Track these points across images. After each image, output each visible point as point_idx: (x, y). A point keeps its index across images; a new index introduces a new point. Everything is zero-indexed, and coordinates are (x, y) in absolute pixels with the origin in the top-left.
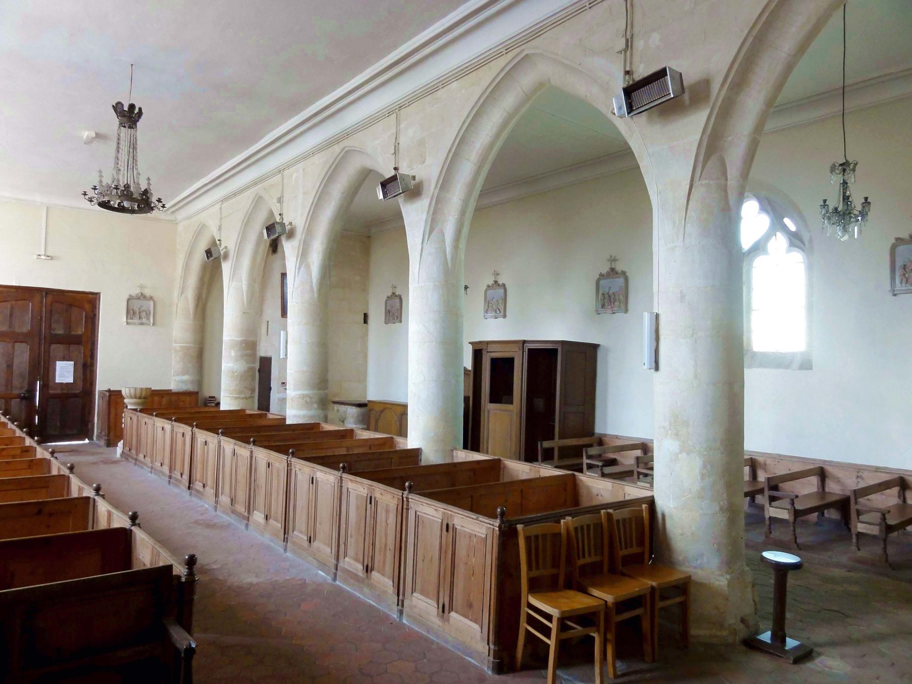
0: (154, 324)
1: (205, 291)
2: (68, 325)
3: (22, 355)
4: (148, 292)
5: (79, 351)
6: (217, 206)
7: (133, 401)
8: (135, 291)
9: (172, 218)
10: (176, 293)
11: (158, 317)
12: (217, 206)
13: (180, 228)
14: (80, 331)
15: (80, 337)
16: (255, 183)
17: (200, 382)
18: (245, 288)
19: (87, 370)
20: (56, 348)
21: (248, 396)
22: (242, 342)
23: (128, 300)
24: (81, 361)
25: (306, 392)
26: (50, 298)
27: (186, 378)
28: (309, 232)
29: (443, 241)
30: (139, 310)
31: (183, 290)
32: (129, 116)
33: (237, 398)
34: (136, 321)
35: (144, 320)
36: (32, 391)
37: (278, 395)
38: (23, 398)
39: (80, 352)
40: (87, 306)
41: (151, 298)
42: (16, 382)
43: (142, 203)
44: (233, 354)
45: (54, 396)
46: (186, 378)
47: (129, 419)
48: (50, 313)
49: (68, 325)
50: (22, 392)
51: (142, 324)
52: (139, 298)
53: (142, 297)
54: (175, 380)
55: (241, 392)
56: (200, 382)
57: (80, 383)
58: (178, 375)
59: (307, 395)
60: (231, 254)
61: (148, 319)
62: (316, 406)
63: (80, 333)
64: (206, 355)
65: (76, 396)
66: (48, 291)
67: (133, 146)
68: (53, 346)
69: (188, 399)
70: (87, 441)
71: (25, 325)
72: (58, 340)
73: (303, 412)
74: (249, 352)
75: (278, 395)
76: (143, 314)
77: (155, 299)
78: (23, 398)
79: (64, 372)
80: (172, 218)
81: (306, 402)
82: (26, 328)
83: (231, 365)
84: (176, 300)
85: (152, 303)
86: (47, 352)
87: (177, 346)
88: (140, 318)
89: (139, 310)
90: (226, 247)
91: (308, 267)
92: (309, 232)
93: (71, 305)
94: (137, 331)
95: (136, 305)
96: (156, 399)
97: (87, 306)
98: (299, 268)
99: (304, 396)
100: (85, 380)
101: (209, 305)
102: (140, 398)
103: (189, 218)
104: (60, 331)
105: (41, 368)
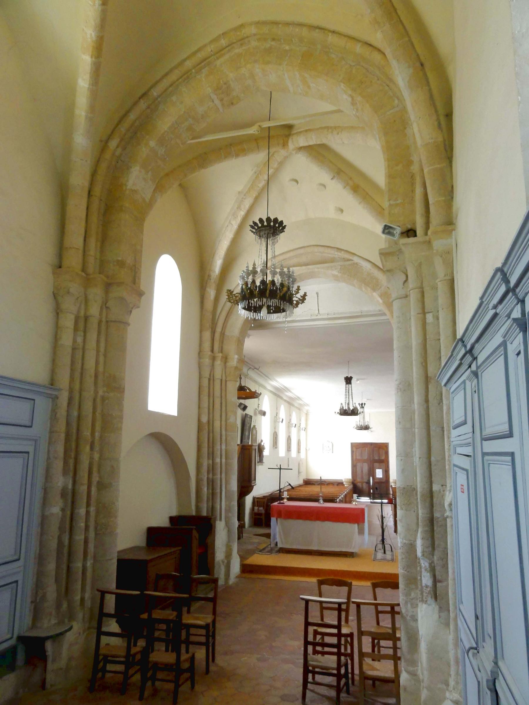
3: (366, 467)
5: (383, 465)
14: (383, 458)
19: (386, 472)
20: (376, 465)
38: (367, 483)
42: (364, 477)
45: (378, 483)
48: (373, 451)
50: (366, 480)
57: (385, 479)
66: (371, 444)
71: (366, 457)
78: (367, 483)
79: (379, 473)
86: (373, 466)
104: (377, 458)
105: (372, 473)
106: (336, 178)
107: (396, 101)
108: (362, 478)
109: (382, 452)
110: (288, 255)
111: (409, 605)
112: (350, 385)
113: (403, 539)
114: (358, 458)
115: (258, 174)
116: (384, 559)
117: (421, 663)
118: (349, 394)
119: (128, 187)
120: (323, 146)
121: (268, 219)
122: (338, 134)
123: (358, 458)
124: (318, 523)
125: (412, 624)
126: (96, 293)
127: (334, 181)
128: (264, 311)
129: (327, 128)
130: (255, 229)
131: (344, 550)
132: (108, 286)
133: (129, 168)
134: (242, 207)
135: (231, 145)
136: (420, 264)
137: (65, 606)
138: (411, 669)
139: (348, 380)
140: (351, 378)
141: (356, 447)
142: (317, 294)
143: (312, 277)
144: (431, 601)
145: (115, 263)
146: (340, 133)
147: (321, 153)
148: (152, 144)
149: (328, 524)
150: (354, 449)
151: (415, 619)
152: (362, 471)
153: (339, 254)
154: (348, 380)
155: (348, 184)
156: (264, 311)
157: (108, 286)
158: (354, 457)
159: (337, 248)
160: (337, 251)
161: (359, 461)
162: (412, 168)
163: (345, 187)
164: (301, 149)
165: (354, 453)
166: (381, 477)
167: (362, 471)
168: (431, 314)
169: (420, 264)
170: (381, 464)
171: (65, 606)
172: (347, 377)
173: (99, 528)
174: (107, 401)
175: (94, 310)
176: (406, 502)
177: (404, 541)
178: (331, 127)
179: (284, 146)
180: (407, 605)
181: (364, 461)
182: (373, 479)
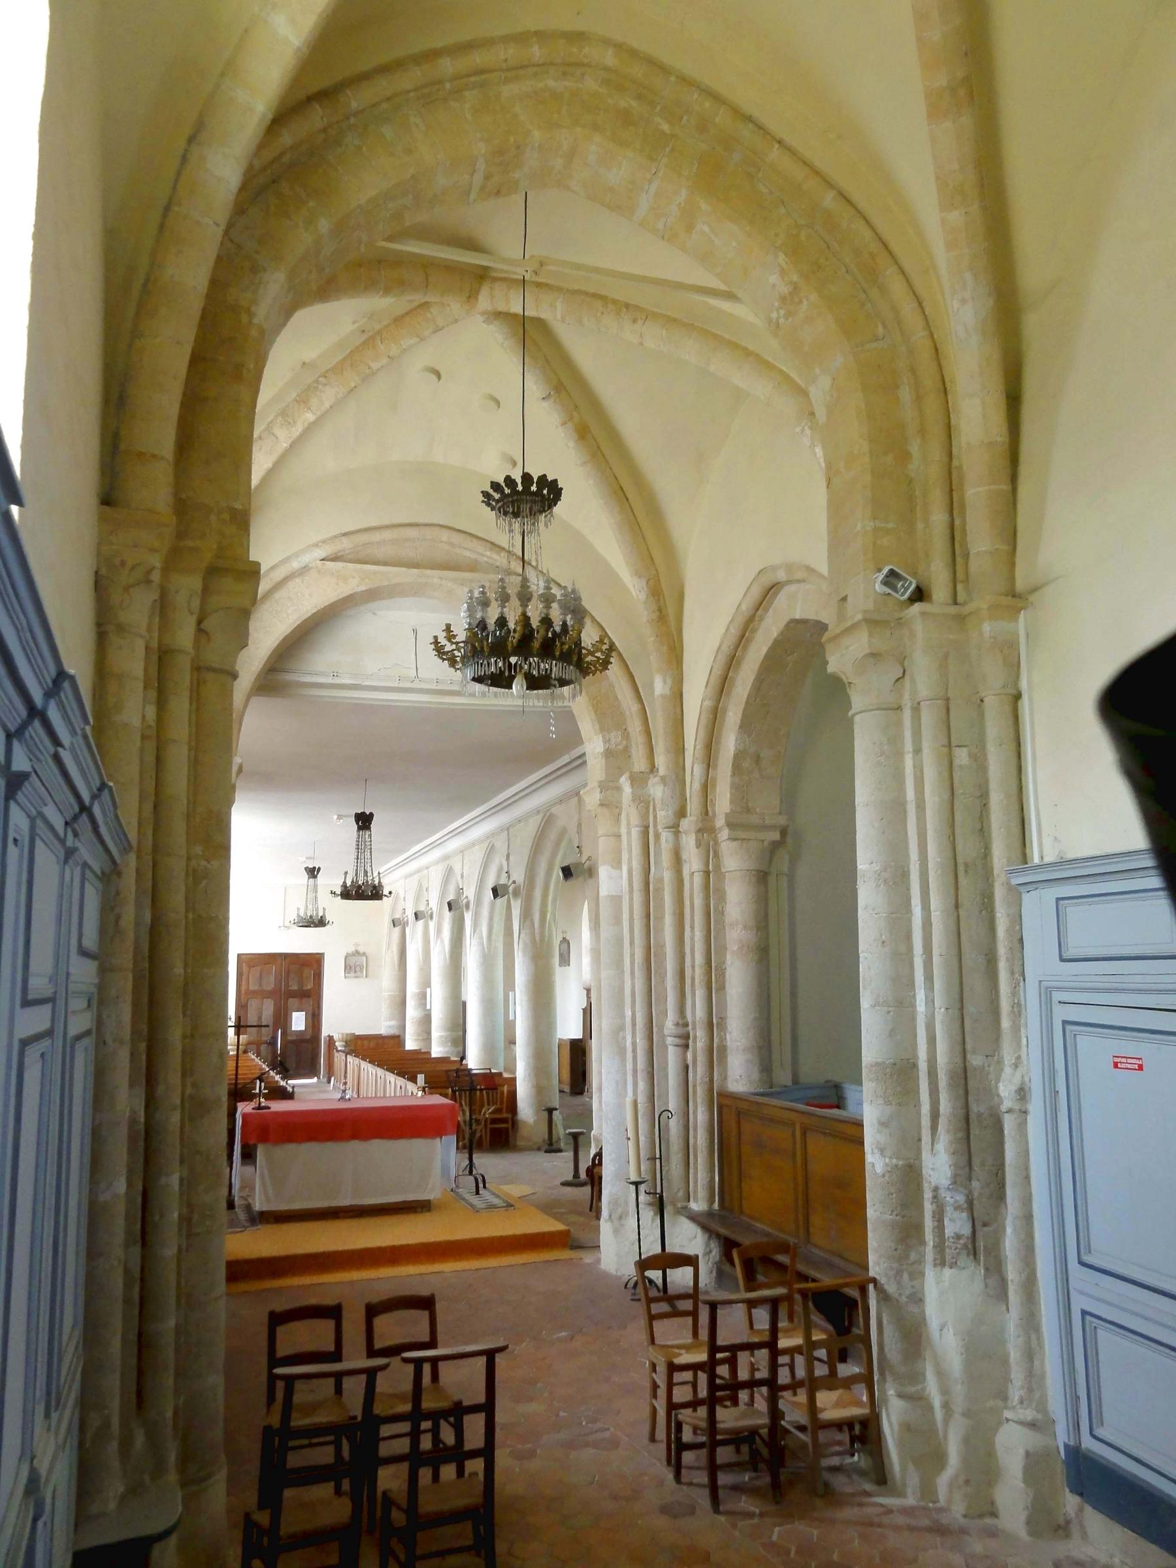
2: (301, 984)
3: (268, 1010)
4: (361, 950)
8: (351, 949)
11: (370, 969)
14: (309, 986)
16: (419, 871)
19: (315, 1019)
20: (292, 1002)
22: (419, 994)
29: (482, 938)
30: (355, 965)
32: (313, 872)
34: (352, 974)
35: (359, 974)
36: (275, 1038)
38: (269, 1044)
43: (321, 923)
45: (292, 1042)
46: (393, 1023)
47: (339, 1058)
48: (288, 973)
49: (301, 984)
53: (357, 953)
54: (384, 1027)
55: (419, 1035)
67: (316, 886)
68: (291, 1000)
69: (392, 1042)
70: (315, 1080)
71: (270, 983)
73: (441, 1049)
78: (269, 1044)
79: (298, 1021)
86: (286, 1004)
87: (386, 994)
89: (355, 965)
91: (442, 941)
95: (352, 960)
96: (359, 1042)
104: (295, 987)
105: (282, 1019)
106: (552, 400)
107: (880, 329)
109: (309, 973)
110: (376, 537)
111: (906, 1276)
112: (368, 833)
113: (891, 1158)
114: (251, 988)
115: (372, 338)
116: (492, 1207)
117: (940, 1374)
118: (362, 848)
119: (255, 321)
120: (540, 323)
121: (527, 478)
122: (634, 321)
124: (355, 1145)
125: (913, 1308)
126: (187, 586)
127: (545, 404)
128: (518, 685)
129: (603, 298)
130: (502, 492)
131: (411, 1197)
132: (213, 572)
133: (255, 269)
134: (314, 402)
135: (379, 262)
136: (946, 656)
137: (140, 1440)
138: (911, 1389)
139: (364, 821)
140: (371, 815)
142: (415, 631)
143: (415, 594)
144: (964, 1260)
145: (226, 516)
146: (640, 322)
147: (530, 336)
148: (324, 225)
149: (378, 1148)
151: (918, 1299)
153: (495, 556)
154: (364, 821)
155: (571, 418)
156: (518, 685)
157: (213, 572)
158: (244, 988)
159: (492, 543)
160: (491, 550)
161: (254, 994)
162: (910, 467)
163: (564, 423)
164: (499, 315)
165: (244, 978)
166: (303, 1028)
168: (965, 749)
169: (946, 656)
170: (304, 1000)
171: (140, 1440)
172: (363, 813)
173: (196, 1217)
174: (204, 883)
175: (184, 636)
176: (899, 1089)
177: (894, 1161)
178: (615, 302)
179: (469, 297)
180: (901, 1277)
181: (263, 994)
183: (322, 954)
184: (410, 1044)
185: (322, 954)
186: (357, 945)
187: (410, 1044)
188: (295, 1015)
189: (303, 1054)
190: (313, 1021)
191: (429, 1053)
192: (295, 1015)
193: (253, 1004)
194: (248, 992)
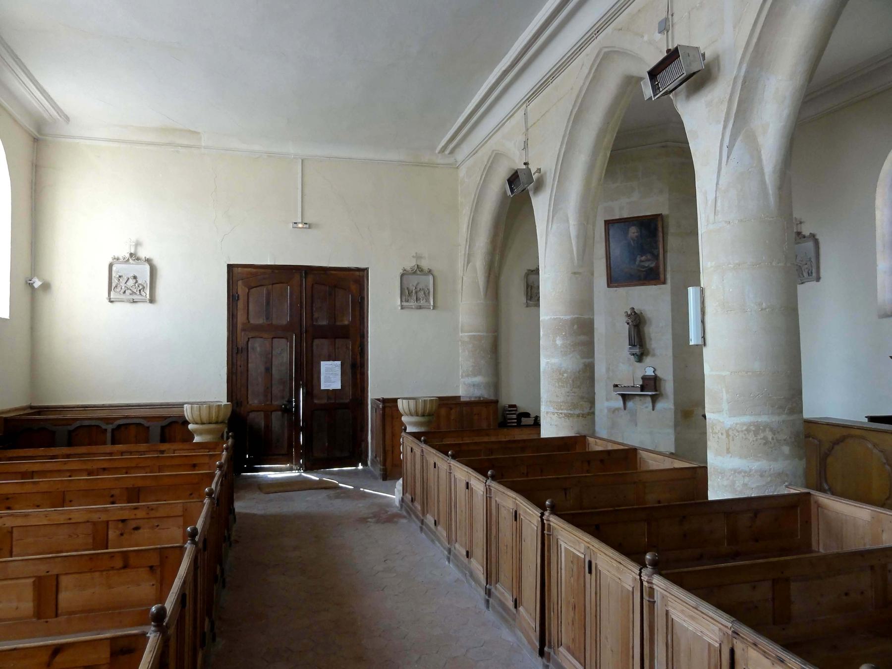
0: (434, 307)
1: (497, 258)
3: (284, 354)
4: (425, 264)
6: (521, 113)
7: (414, 419)
8: (410, 264)
9: (451, 160)
10: (460, 264)
12: (521, 113)
13: (462, 172)
15: (346, 327)
17: (496, 385)
18: (573, 232)
19: (356, 371)
21: (587, 411)
23: (402, 276)
24: (349, 362)
25: (764, 419)
26: (310, 278)
27: (478, 379)
28: (759, 54)
30: (416, 288)
31: (469, 259)
33: (568, 416)
34: (412, 303)
35: (422, 302)
37: (607, 404)
39: (347, 348)
40: (353, 287)
41: (430, 272)
42: (276, 390)
44: (559, 342)
46: (478, 379)
47: (410, 449)
51: (420, 308)
52: (415, 273)
53: (418, 270)
54: (465, 384)
55: (574, 406)
56: (496, 385)
57: (349, 391)
58: (468, 376)
59: (766, 426)
60: (549, 181)
61: (427, 300)
62: (786, 449)
63: (346, 323)
64: (503, 350)
65: (345, 406)
68: (317, 342)
72: (320, 333)
74: (583, 338)
75: (607, 404)
76: (421, 294)
77: (435, 273)
79: (331, 375)
80: (451, 160)
81: (764, 441)
82: (285, 320)
83: (555, 360)
84: (460, 273)
85: (431, 278)
87: (465, 336)
88: (417, 299)
89: (416, 288)
90: (539, 170)
92: (759, 54)
93: (335, 286)
94: (414, 317)
95: (412, 281)
97: (353, 287)
98: (730, 147)
99: (757, 428)
100: (354, 385)
101: (503, 278)
102: (423, 415)
103: (475, 152)
108: (268, 390)
123: (257, 320)
141: (248, 285)
150: (241, 289)
152: (268, 370)
158: (241, 318)
165: (241, 304)
166: (337, 386)
167: (268, 370)
170: (339, 342)
181: (277, 332)
182: (308, 395)
183: (366, 270)
184: (552, 427)
185: (366, 270)
186: (418, 257)
187: (552, 427)
188: (325, 365)
189: (339, 431)
190: (354, 374)
191: (698, 476)
192: (325, 365)
193: (258, 347)
194: (250, 328)
